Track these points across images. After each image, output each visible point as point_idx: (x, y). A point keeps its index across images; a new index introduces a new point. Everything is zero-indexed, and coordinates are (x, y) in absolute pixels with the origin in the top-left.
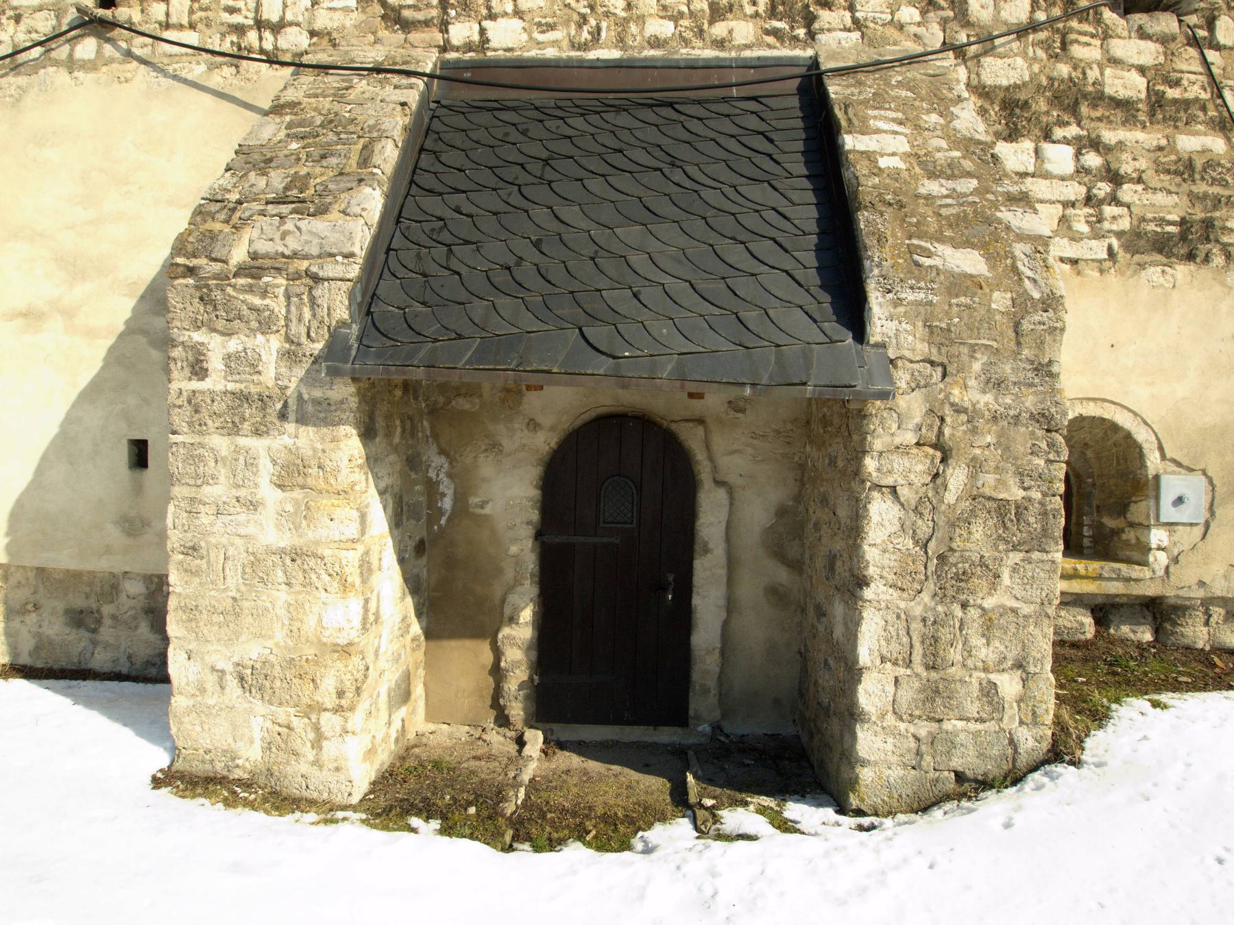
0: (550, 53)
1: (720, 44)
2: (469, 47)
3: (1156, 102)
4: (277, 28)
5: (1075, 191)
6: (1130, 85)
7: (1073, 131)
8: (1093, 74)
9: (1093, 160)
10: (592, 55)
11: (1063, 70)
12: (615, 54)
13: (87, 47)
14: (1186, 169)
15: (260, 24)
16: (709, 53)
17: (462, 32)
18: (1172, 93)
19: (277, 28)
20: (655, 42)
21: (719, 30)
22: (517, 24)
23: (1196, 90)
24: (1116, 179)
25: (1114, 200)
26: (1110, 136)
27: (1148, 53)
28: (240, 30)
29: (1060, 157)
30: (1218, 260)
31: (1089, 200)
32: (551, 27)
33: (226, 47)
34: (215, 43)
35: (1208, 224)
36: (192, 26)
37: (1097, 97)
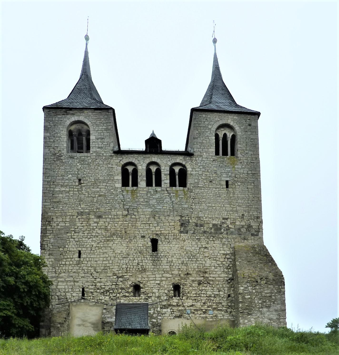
0: (126, 303)
1: (140, 302)
2: (119, 302)
3: (177, 305)
4: (101, 300)
5: (170, 313)
6: (175, 304)
7: (170, 308)
8: (172, 303)
9: (172, 310)
10: (130, 303)
11: (169, 303)
12: (132, 303)
13: (82, 301)
14: (180, 311)
15: (100, 299)
16: (140, 303)
17: (118, 301)
18: (179, 304)
19: (101, 300)
20: (135, 302)
21: (140, 301)
22: (123, 300)
23: (180, 304)
24: (174, 312)
25: (173, 313)
26: (173, 308)
27: (177, 301)
28: (98, 300)
29: (169, 310)
30: (183, 318)
31: (171, 314)
32: (126, 300)
33: (97, 301)
34: (95, 301)
35: (182, 315)
36: (93, 299)
37: (172, 305)
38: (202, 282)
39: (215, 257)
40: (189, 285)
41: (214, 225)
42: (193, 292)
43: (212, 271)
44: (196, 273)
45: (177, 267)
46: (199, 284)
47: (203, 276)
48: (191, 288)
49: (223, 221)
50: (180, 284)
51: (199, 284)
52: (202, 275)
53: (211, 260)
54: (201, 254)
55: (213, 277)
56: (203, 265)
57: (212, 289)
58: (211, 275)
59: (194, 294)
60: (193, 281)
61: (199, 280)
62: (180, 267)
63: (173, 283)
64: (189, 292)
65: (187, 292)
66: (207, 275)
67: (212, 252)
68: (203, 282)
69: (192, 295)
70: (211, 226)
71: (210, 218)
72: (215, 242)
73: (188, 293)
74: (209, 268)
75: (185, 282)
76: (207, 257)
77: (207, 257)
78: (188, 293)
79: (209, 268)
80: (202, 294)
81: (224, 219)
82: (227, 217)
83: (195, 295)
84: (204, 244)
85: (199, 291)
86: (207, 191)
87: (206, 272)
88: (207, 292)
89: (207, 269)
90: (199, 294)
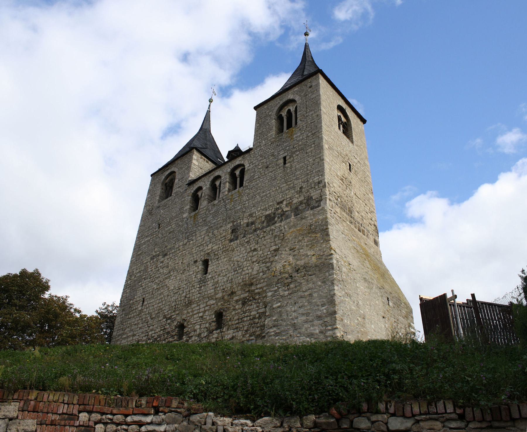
38: (246, 300)
39: (265, 258)
40: (232, 308)
41: (266, 216)
42: (236, 318)
43: (260, 280)
44: (242, 289)
45: (222, 288)
46: (244, 304)
47: (249, 291)
48: (233, 313)
49: (278, 206)
50: (222, 311)
51: (244, 304)
52: (247, 290)
53: (259, 264)
54: (249, 261)
55: (260, 288)
56: (250, 275)
57: (258, 307)
58: (258, 286)
59: (236, 320)
60: (237, 301)
61: (243, 298)
62: (224, 287)
63: (216, 311)
64: (231, 319)
65: (228, 320)
66: (253, 288)
67: (261, 252)
68: (248, 299)
69: (233, 322)
70: (263, 219)
71: (263, 210)
72: (266, 238)
73: (230, 320)
74: (256, 276)
75: (228, 306)
76: (256, 262)
77: (256, 262)
78: (230, 320)
79: (256, 276)
80: (245, 317)
81: (278, 203)
82: (282, 200)
83: (237, 321)
84: (253, 246)
85: (242, 314)
86: (262, 179)
87: (252, 284)
88: (251, 312)
89: (253, 278)
90: (242, 319)
